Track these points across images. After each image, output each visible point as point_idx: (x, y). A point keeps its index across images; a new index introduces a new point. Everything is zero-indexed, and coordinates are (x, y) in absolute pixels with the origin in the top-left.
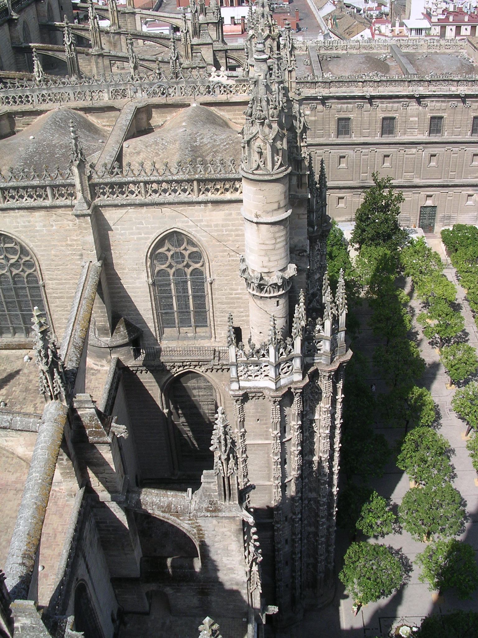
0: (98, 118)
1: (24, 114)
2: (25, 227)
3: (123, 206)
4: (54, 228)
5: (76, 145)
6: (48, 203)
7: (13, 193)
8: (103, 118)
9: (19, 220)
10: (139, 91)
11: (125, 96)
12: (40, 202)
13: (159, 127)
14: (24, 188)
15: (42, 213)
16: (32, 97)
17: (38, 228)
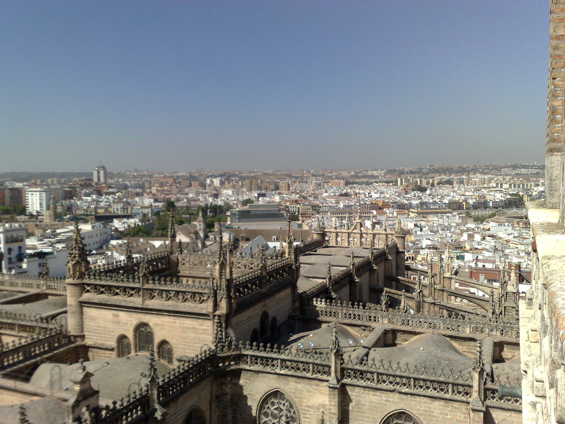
0: (460, 345)
1: (405, 332)
2: (425, 411)
3: (508, 410)
4: (448, 416)
5: (480, 357)
6: (447, 396)
7: (422, 383)
8: (464, 346)
9: (422, 405)
10: (495, 330)
11: (482, 332)
12: (441, 394)
13: (508, 359)
14: (432, 381)
15: (442, 403)
16: (412, 321)
17: (435, 414)
